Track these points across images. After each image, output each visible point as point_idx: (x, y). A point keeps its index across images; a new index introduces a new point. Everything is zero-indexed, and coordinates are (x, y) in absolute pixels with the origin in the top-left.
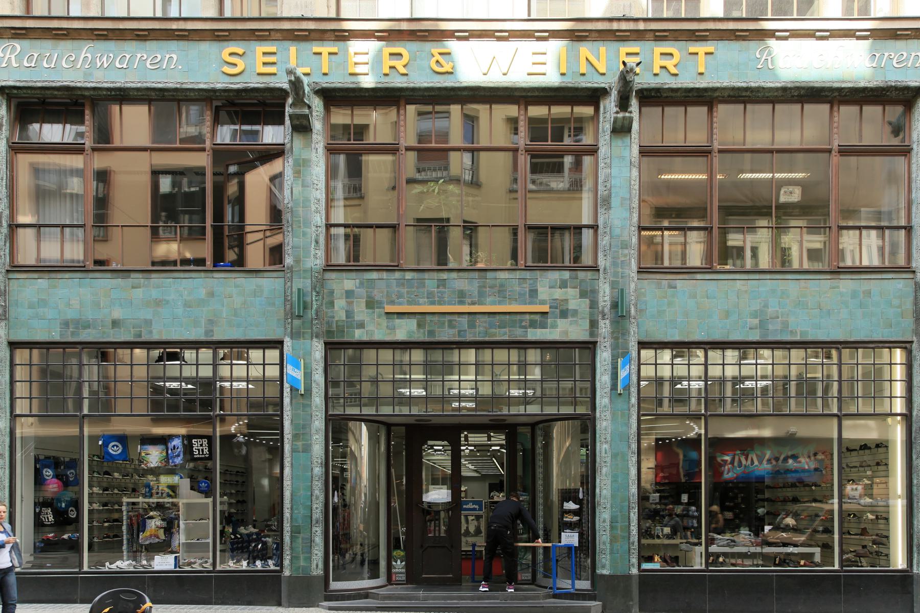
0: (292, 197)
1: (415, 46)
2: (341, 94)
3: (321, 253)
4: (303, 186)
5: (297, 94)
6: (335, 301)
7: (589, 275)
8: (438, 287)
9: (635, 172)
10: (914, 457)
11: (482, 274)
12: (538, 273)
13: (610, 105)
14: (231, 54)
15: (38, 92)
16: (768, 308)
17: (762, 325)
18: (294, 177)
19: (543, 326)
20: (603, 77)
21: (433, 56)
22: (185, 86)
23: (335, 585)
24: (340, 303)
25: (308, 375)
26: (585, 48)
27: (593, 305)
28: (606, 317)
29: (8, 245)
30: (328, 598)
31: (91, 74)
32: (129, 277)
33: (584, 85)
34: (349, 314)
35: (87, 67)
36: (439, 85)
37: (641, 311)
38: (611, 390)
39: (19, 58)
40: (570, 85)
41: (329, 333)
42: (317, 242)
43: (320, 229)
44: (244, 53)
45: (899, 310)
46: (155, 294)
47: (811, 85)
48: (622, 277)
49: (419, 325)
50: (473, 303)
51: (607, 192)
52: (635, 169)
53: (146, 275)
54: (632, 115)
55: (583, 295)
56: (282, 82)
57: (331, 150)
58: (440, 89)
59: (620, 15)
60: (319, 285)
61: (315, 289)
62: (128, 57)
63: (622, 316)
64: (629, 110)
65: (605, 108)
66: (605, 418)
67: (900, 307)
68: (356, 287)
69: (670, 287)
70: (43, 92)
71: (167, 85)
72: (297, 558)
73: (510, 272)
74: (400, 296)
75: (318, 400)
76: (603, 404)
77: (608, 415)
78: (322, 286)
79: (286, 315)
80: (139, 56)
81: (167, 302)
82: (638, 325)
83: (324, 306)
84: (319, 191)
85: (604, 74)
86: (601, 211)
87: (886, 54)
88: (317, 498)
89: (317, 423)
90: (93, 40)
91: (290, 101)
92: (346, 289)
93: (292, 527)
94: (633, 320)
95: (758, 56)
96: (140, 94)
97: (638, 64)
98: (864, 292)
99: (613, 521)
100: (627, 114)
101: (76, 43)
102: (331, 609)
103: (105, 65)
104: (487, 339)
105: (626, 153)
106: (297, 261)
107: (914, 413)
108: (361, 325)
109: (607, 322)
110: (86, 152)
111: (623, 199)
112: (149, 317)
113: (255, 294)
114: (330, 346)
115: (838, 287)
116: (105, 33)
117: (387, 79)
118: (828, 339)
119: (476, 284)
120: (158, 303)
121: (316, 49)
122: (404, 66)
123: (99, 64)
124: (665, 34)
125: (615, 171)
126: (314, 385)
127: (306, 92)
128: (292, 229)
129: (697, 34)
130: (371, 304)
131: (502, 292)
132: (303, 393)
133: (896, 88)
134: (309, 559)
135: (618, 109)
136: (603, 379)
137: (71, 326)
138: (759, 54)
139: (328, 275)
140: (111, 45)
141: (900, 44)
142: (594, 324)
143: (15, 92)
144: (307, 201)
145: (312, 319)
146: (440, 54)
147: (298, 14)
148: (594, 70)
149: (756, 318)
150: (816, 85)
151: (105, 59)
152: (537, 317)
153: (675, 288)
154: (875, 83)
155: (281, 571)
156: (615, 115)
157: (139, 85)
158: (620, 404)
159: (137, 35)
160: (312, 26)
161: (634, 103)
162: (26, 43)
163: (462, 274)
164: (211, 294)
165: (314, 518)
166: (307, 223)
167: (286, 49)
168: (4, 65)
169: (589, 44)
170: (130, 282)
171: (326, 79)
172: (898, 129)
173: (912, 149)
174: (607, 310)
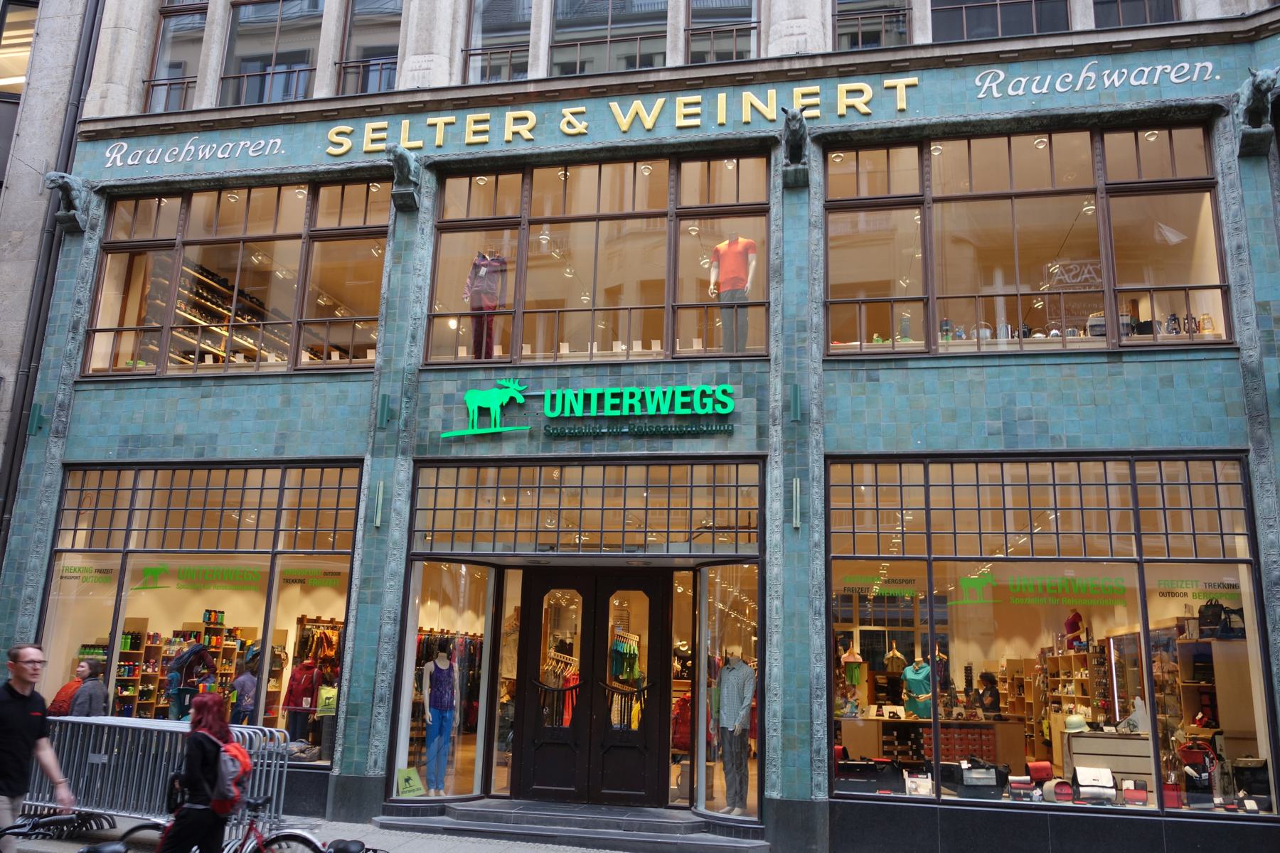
0: (389, 286)
1: (545, 108)
2: (456, 166)
3: (418, 350)
4: (403, 272)
6: (431, 408)
7: (757, 367)
10: (1270, 628)
11: (616, 369)
12: (688, 366)
14: (338, 134)
15: (138, 189)
16: (1015, 405)
17: (1008, 428)
18: (395, 263)
20: (773, 124)
21: (564, 116)
22: (286, 171)
24: (436, 411)
26: (749, 93)
27: (762, 405)
28: (777, 422)
29: (81, 353)
31: (191, 167)
32: (199, 385)
33: (747, 135)
35: (188, 159)
36: (569, 149)
37: (830, 412)
38: (784, 522)
40: (730, 136)
42: (413, 337)
43: (419, 322)
44: (352, 131)
45: (1221, 404)
46: (225, 404)
47: (1055, 112)
48: (799, 369)
51: (779, 260)
52: (816, 231)
53: (218, 382)
54: (807, 167)
58: (570, 152)
59: (792, 53)
60: (413, 390)
61: (406, 394)
62: (231, 145)
64: (803, 161)
65: (776, 160)
66: (776, 562)
67: (1222, 399)
68: (458, 391)
69: (870, 379)
70: (143, 189)
71: (267, 171)
73: (651, 366)
76: (774, 542)
78: (417, 389)
79: (370, 427)
80: (242, 143)
81: (238, 413)
82: (824, 433)
83: (417, 414)
84: (421, 278)
85: (773, 121)
86: (773, 284)
87: (1160, 68)
90: (199, 132)
92: (444, 392)
94: (816, 426)
95: (978, 83)
96: (239, 182)
98: (1161, 380)
100: (800, 166)
101: (181, 137)
103: (207, 157)
105: (804, 212)
106: (388, 361)
107: (1262, 559)
109: (779, 428)
110: (176, 248)
111: (800, 269)
112: (216, 431)
114: (419, 464)
115: (1121, 373)
116: (211, 124)
120: (227, 414)
121: (431, 120)
123: (201, 156)
124: (851, 69)
125: (788, 235)
126: (393, 515)
127: (412, 168)
128: (386, 323)
129: (893, 65)
132: (378, 524)
135: (788, 161)
137: (130, 444)
138: (980, 80)
139: (424, 377)
142: (762, 432)
143: (116, 190)
144: (405, 288)
145: (399, 431)
146: (573, 114)
147: (413, 86)
148: (761, 118)
149: (998, 419)
150: (1061, 112)
151: (207, 150)
153: (878, 380)
154: (1147, 104)
156: (784, 168)
157: (238, 174)
159: (243, 123)
160: (427, 97)
161: (812, 152)
163: (588, 370)
166: (403, 316)
167: (398, 124)
168: (109, 165)
169: (756, 88)
170: (200, 390)
171: (440, 152)
173: (1217, 182)
174: (778, 413)
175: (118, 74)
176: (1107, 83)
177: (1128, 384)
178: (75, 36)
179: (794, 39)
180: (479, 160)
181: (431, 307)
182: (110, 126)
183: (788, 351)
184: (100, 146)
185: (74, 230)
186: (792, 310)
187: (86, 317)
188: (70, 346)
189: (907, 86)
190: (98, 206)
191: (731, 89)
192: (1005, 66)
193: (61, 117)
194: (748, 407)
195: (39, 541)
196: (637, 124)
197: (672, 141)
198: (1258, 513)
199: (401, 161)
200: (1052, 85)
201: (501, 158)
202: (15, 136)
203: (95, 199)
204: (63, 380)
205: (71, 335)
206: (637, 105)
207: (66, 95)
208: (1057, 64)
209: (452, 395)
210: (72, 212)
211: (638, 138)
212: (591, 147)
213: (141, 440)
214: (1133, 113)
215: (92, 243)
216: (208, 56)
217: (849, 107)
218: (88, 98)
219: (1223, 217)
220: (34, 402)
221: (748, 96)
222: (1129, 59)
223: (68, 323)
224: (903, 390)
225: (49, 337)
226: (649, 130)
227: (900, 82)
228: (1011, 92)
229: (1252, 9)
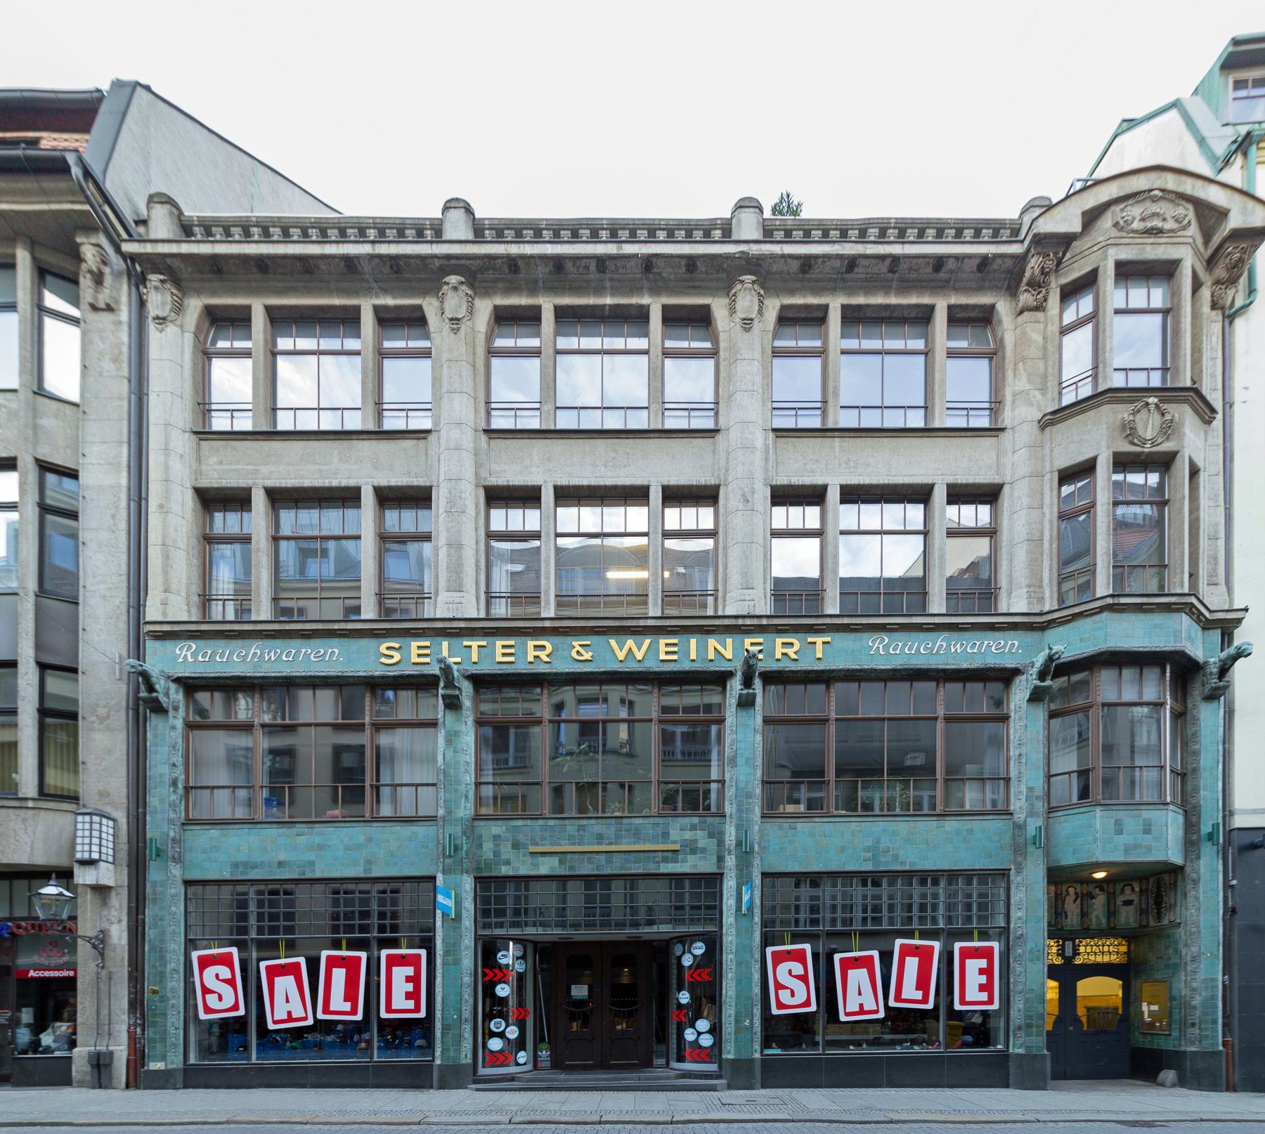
1: (558, 640)
4: (454, 752)
5: (447, 678)
7: (717, 820)
8: (578, 831)
9: (759, 738)
10: (1011, 960)
11: (619, 820)
13: (735, 685)
14: (388, 648)
19: (675, 861)
22: (345, 674)
23: (483, 1071)
24: (488, 846)
25: (458, 903)
27: (721, 843)
29: (183, 802)
30: (475, 1082)
33: (712, 669)
34: (496, 854)
39: (194, 655)
41: (478, 869)
44: (400, 647)
46: (317, 840)
49: (561, 862)
50: (611, 844)
55: (711, 835)
56: (435, 670)
57: (479, 723)
58: (580, 673)
59: (745, 613)
63: (746, 852)
67: (1000, 841)
69: (791, 828)
72: (448, 1050)
74: (543, 838)
75: (468, 922)
77: (733, 931)
78: (472, 831)
79: (438, 855)
80: (304, 651)
81: (330, 846)
85: (730, 660)
87: (986, 643)
88: (466, 1001)
89: (466, 941)
91: (442, 684)
93: (442, 1025)
97: (760, 651)
99: (738, 1015)
101: (246, 642)
102: (478, 1090)
104: (623, 872)
105: (751, 722)
106: (449, 812)
108: (508, 863)
109: (733, 857)
111: (747, 759)
113: (410, 839)
117: (531, 666)
118: (935, 868)
119: (613, 828)
120: (321, 847)
122: (548, 656)
130: (516, 846)
131: (637, 835)
133: (994, 669)
134: (458, 1051)
136: (729, 902)
139: (477, 823)
140: (278, 642)
141: (997, 634)
142: (720, 859)
144: (457, 763)
146: (580, 645)
152: (669, 854)
155: (433, 1061)
157: (304, 674)
158: (744, 922)
160: (462, 625)
161: (758, 683)
162: (201, 643)
163: (599, 821)
164: (370, 840)
165: (463, 1017)
166: (458, 782)
168: (181, 660)
169: (718, 636)
172: (998, 703)
174: (732, 848)
175: (174, 587)
176: (953, 650)
177: (947, 832)
178: (124, 548)
179: (746, 603)
180: (508, 675)
181: (476, 778)
182: (176, 628)
183: (739, 810)
184: (169, 644)
185: (159, 709)
186: (742, 785)
187: (183, 777)
188: (173, 797)
189: (824, 643)
190: (177, 692)
191: (699, 636)
192: (889, 634)
193: (125, 618)
194: (711, 844)
195: (174, 932)
196: (629, 657)
197: (657, 669)
198: (1012, 902)
199: (447, 670)
200: (918, 649)
201: (525, 674)
202: (80, 630)
203: (173, 687)
204: (171, 821)
205: (172, 789)
206: (630, 643)
207: (126, 600)
208: (922, 635)
209: (500, 836)
210: (154, 694)
211: (632, 666)
212: (596, 670)
213: (247, 866)
214: (967, 670)
215: (177, 721)
216: (259, 578)
217: (783, 654)
218: (148, 603)
219: (1012, 737)
220: (148, 837)
221: (712, 642)
222: (967, 635)
223: (167, 780)
224: (812, 835)
225: (152, 791)
226: (639, 661)
227: (819, 640)
228: (891, 652)
229: (1047, 609)
